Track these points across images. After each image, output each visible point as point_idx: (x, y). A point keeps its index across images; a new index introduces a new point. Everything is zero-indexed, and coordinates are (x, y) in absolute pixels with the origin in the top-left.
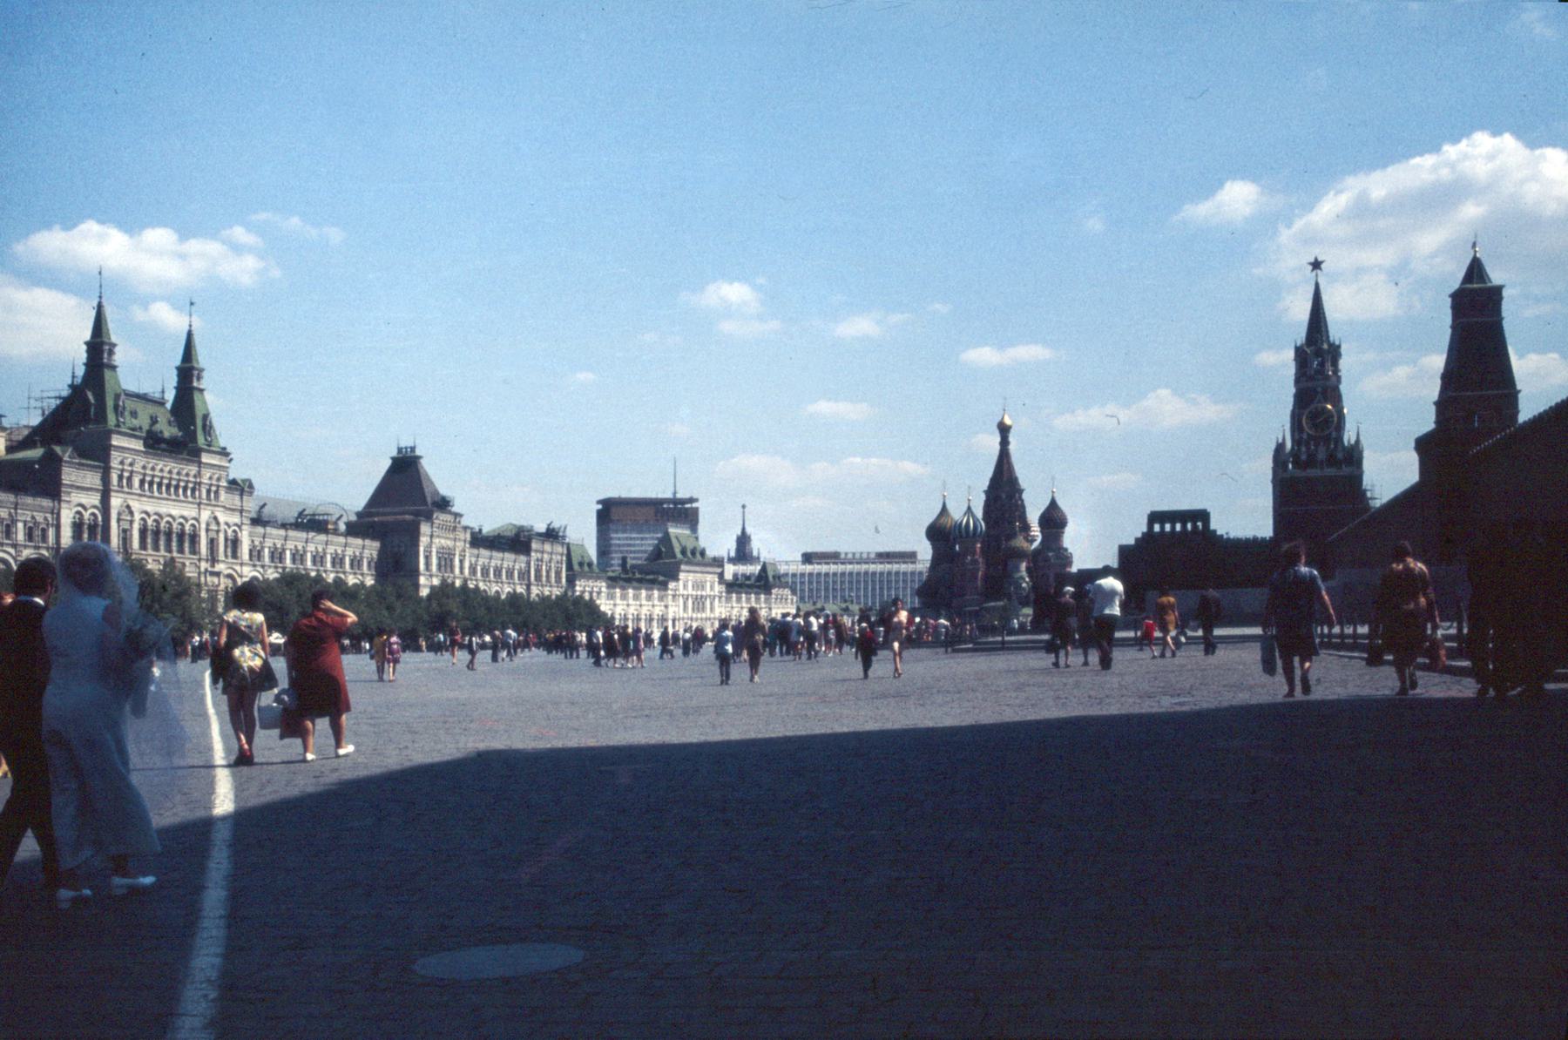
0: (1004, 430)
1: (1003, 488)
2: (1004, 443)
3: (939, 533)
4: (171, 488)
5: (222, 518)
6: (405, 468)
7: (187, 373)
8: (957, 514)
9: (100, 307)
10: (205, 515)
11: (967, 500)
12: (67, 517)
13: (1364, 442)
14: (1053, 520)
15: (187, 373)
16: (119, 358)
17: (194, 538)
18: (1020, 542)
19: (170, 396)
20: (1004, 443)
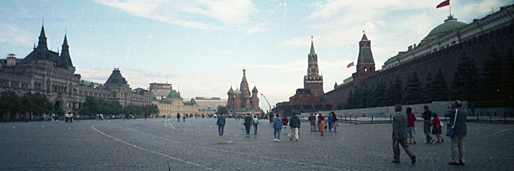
0: (244, 71)
1: (244, 83)
2: (244, 74)
3: (230, 93)
5: (73, 83)
6: (116, 72)
7: (65, 47)
10: (69, 83)
11: (236, 87)
12: (33, 82)
13: (323, 76)
14: (255, 91)
15: (65, 47)
16: (48, 41)
17: (65, 88)
18: (247, 96)
19: (60, 52)
20: (244, 74)
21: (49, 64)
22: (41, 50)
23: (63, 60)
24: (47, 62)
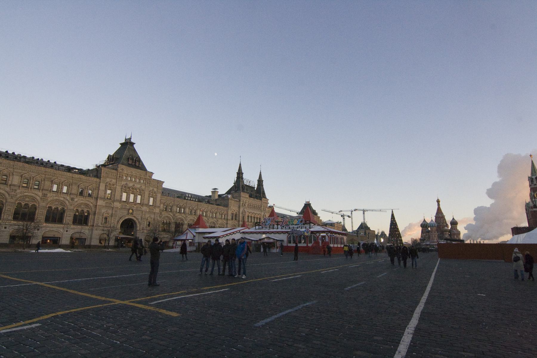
0: (438, 201)
1: (439, 215)
2: (439, 205)
3: (424, 226)
4: (254, 207)
6: (307, 206)
7: (260, 182)
8: (428, 220)
9: (240, 164)
10: (263, 213)
11: (430, 217)
14: (454, 223)
16: (244, 176)
19: (256, 186)
20: (439, 205)
21: (244, 196)
22: (239, 186)
23: (258, 193)
24: (242, 194)
